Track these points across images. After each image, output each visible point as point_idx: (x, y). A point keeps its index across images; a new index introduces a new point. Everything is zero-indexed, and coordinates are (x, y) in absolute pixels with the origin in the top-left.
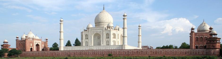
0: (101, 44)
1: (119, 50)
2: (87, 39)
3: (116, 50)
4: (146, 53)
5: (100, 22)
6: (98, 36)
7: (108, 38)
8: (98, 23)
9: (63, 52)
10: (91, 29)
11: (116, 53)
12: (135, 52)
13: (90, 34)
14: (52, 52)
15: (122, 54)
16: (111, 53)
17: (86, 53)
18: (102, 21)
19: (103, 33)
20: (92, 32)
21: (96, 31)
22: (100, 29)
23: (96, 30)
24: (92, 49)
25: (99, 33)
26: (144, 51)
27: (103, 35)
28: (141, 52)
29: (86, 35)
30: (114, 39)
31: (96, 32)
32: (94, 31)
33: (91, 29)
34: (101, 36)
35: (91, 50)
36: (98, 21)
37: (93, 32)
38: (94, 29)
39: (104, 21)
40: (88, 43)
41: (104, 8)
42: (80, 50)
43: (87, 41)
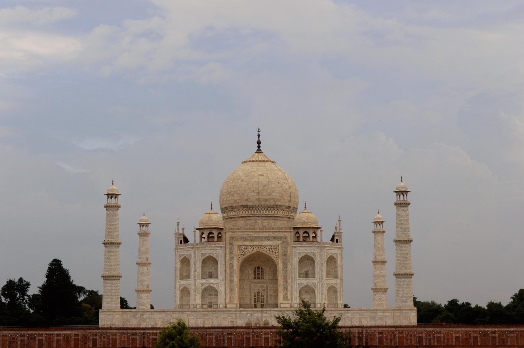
0: (281, 300)
1: (394, 329)
2: (211, 276)
3: (381, 330)
4: (503, 341)
5: (257, 203)
6: (259, 266)
7: (306, 275)
8: (246, 206)
9: (136, 334)
10: (234, 235)
11: (381, 340)
12: (457, 338)
13: (227, 258)
14: (77, 335)
15: (404, 344)
16: (360, 339)
17: (248, 339)
18: (266, 200)
19: (285, 255)
20: (236, 248)
21: (256, 243)
22: (272, 235)
23: (255, 239)
24: (262, 325)
25: (268, 253)
26: (494, 332)
27: (285, 264)
28: (481, 336)
29: (210, 261)
30: (332, 281)
31: (255, 250)
32: (247, 243)
33: (234, 235)
34: (280, 266)
35: (259, 328)
36: (246, 200)
37: (239, 247)
38: (245, 235)
39: (273, 203)
40: (217, 295)
41: (259, 143)
42: (207, 326)
43: (215, 286)
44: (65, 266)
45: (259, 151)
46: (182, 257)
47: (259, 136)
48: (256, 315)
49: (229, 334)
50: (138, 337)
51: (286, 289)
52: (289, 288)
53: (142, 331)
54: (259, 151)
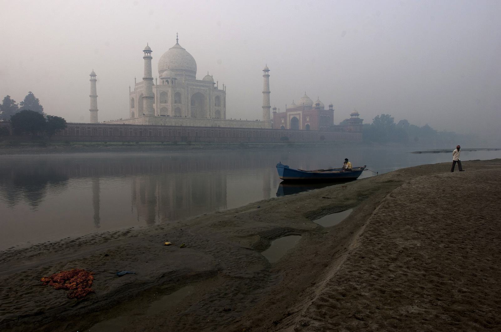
8: (182, 70)
13: (186, 94)
21: (198, 88)
32: (194, 87)
41: (177, 40)
44: (36, 96)
45: (177, 44)
46: (161, 92)
47: (177, 36)
48: (215, 122)
49: (212, 130)
50: (172, 131)
51: (210, 111)
52: (211, 111)
53: (174, 128)
54: (177, 44)
